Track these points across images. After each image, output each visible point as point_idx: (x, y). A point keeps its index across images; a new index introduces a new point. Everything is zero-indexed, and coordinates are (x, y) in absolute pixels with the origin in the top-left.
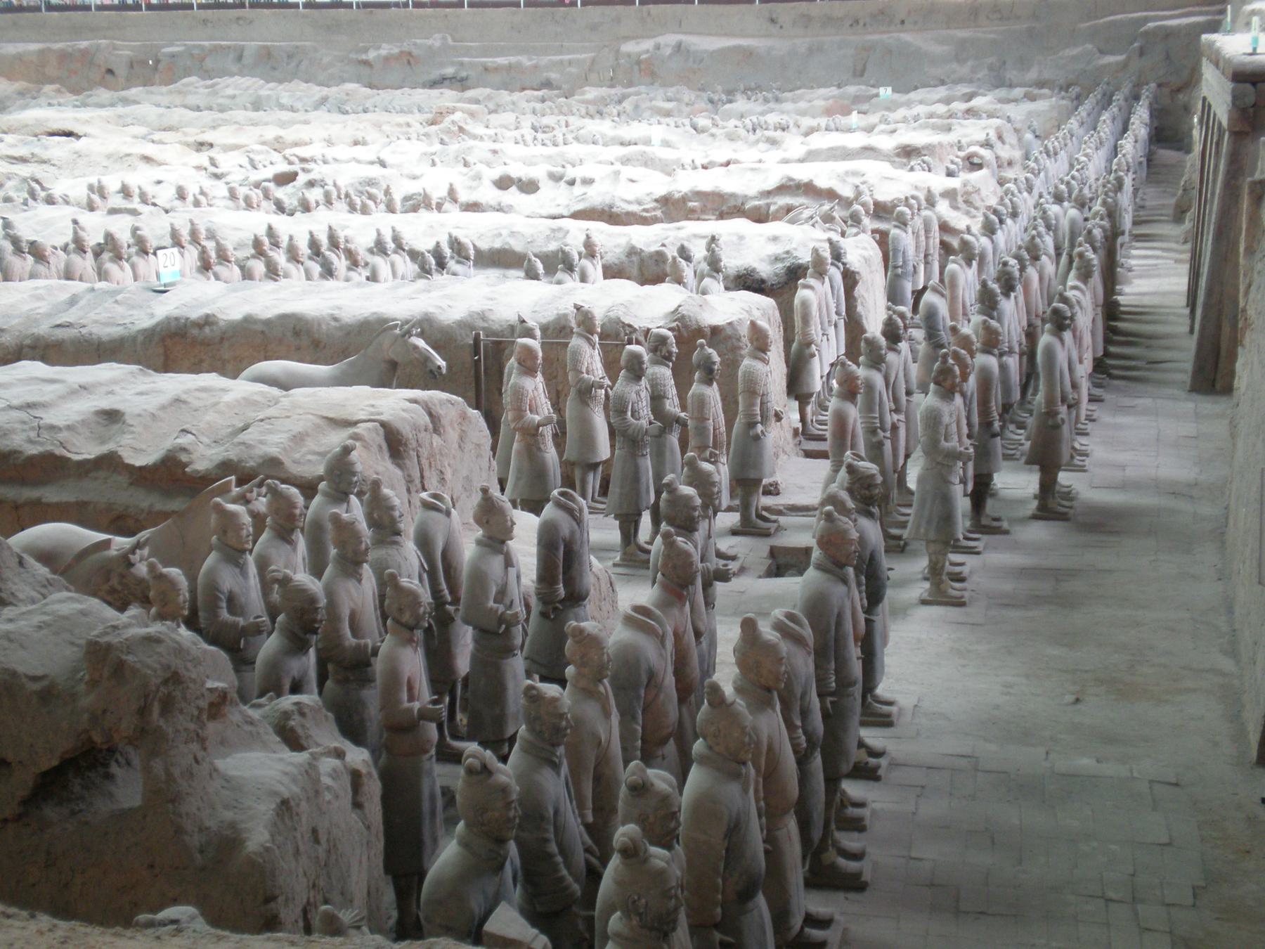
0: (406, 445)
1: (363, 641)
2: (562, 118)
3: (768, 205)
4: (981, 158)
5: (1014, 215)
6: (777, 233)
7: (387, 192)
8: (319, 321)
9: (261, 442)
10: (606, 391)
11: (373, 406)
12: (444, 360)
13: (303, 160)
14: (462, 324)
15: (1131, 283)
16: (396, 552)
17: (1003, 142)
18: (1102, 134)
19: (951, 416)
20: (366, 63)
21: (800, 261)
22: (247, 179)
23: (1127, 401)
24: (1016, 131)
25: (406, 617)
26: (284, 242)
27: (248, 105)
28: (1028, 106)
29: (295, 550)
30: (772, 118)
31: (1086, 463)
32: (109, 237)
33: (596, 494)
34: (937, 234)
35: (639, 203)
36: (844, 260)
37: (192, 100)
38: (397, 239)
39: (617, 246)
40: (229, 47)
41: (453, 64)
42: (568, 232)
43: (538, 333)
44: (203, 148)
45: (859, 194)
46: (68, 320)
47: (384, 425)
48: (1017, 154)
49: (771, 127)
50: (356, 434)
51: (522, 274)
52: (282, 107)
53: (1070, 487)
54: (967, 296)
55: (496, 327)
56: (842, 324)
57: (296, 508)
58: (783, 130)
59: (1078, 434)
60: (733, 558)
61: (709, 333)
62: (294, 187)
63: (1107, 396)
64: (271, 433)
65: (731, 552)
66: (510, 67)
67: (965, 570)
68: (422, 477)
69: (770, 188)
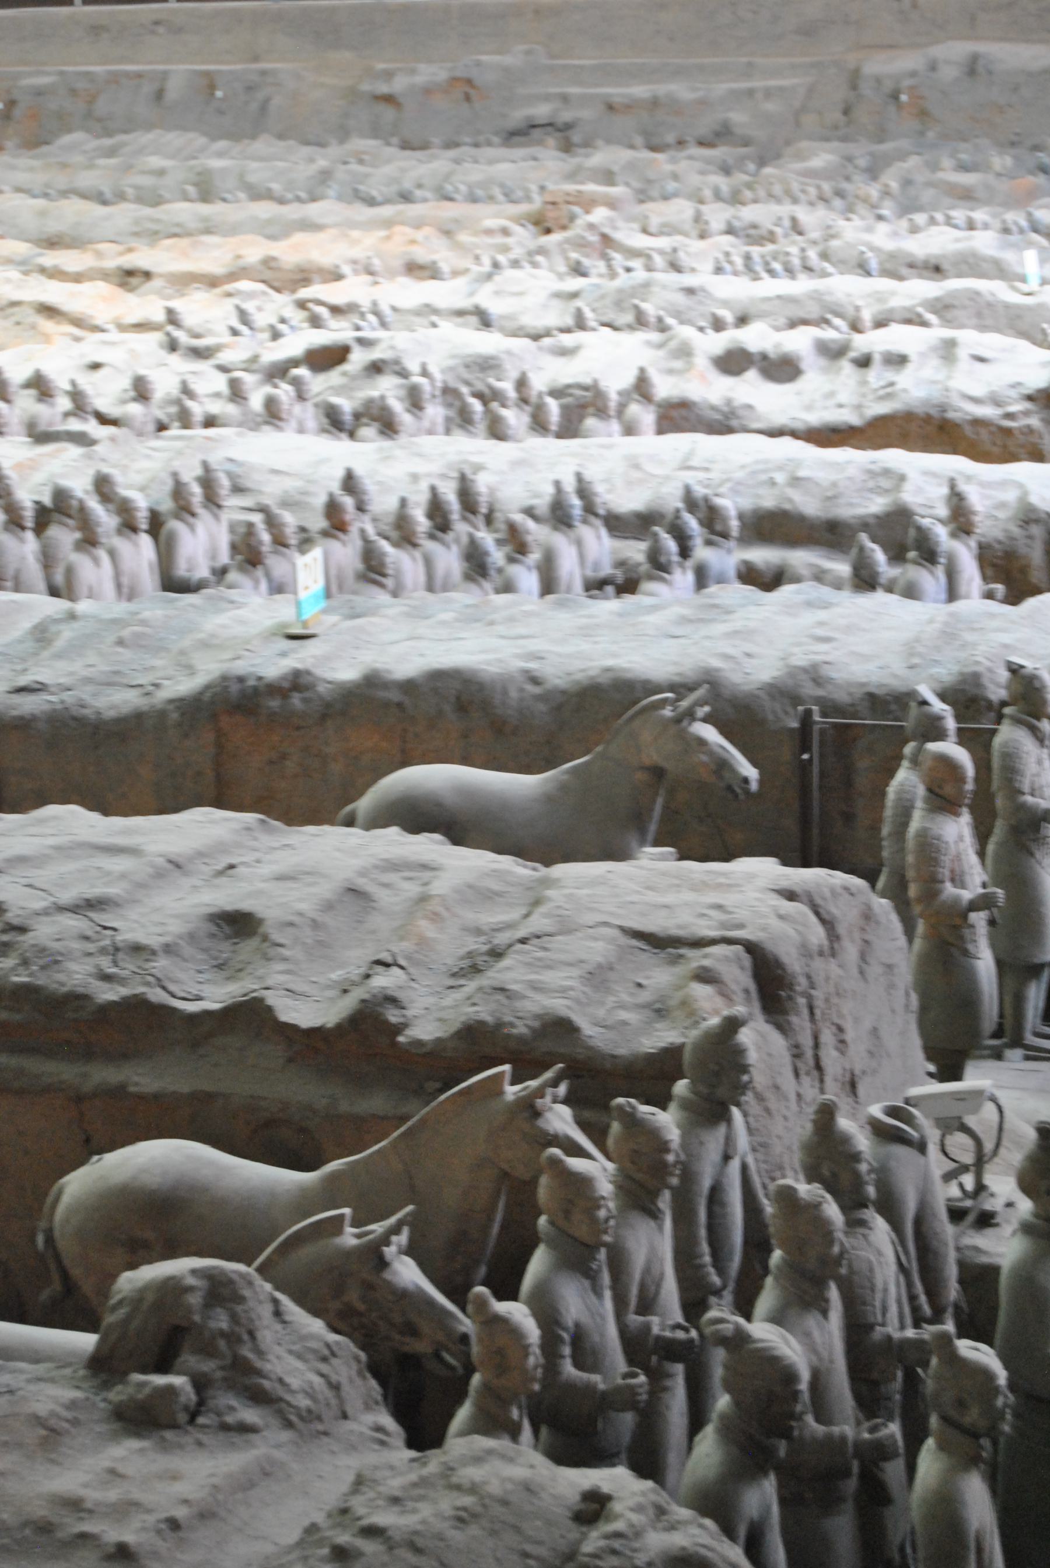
0: (790, 987)
1: (836, 1430)
2: (785, 210)
7: (522, 384)
8: (504, 683)
9: (536, 987)
11: (719, 907)
12: (755, 763)
13: (336, 310)
16: (862, 1242)
20: (389, 99)
22: (255, 359)
25: (973, 1416)
26: (384, 504)
27: (191, 190)
29: (661, 1228)
32: (61, 496)
33: (1038, 1021)
35: (996, 401)
37: (87, 179)
38: (584, 491)
39: (1002, 505)
40: (139, 75)
41: (547, 98)
42: (902, 478)
43: (951, 724)
44: (134, 281)
46: (40, 678)
47: (751, 948)
50: (704, 969)
51: (842, 568)
52: (258, 194)
55: (842, 697)
57: (667, 1150)
62: (344, 374)
64: (549, 967)
66: (655, 103)
68: (817, 1045)
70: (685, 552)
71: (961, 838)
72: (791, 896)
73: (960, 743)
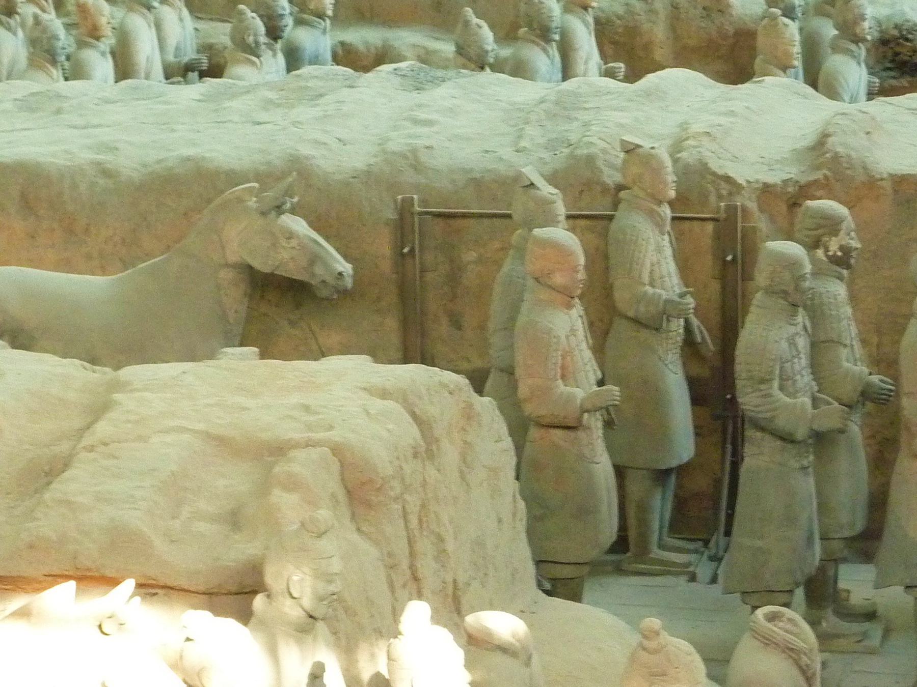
10: (687, 321)
11: (307, 408)
14: (368, 176)
33: (666, 530)
43: (561, 210)
51: (447, 48)
61: (889, 190)
68: (412, 554)
70: (274, 33)
71: (573, 331)
72: (384, 394)
73: (572, 229)
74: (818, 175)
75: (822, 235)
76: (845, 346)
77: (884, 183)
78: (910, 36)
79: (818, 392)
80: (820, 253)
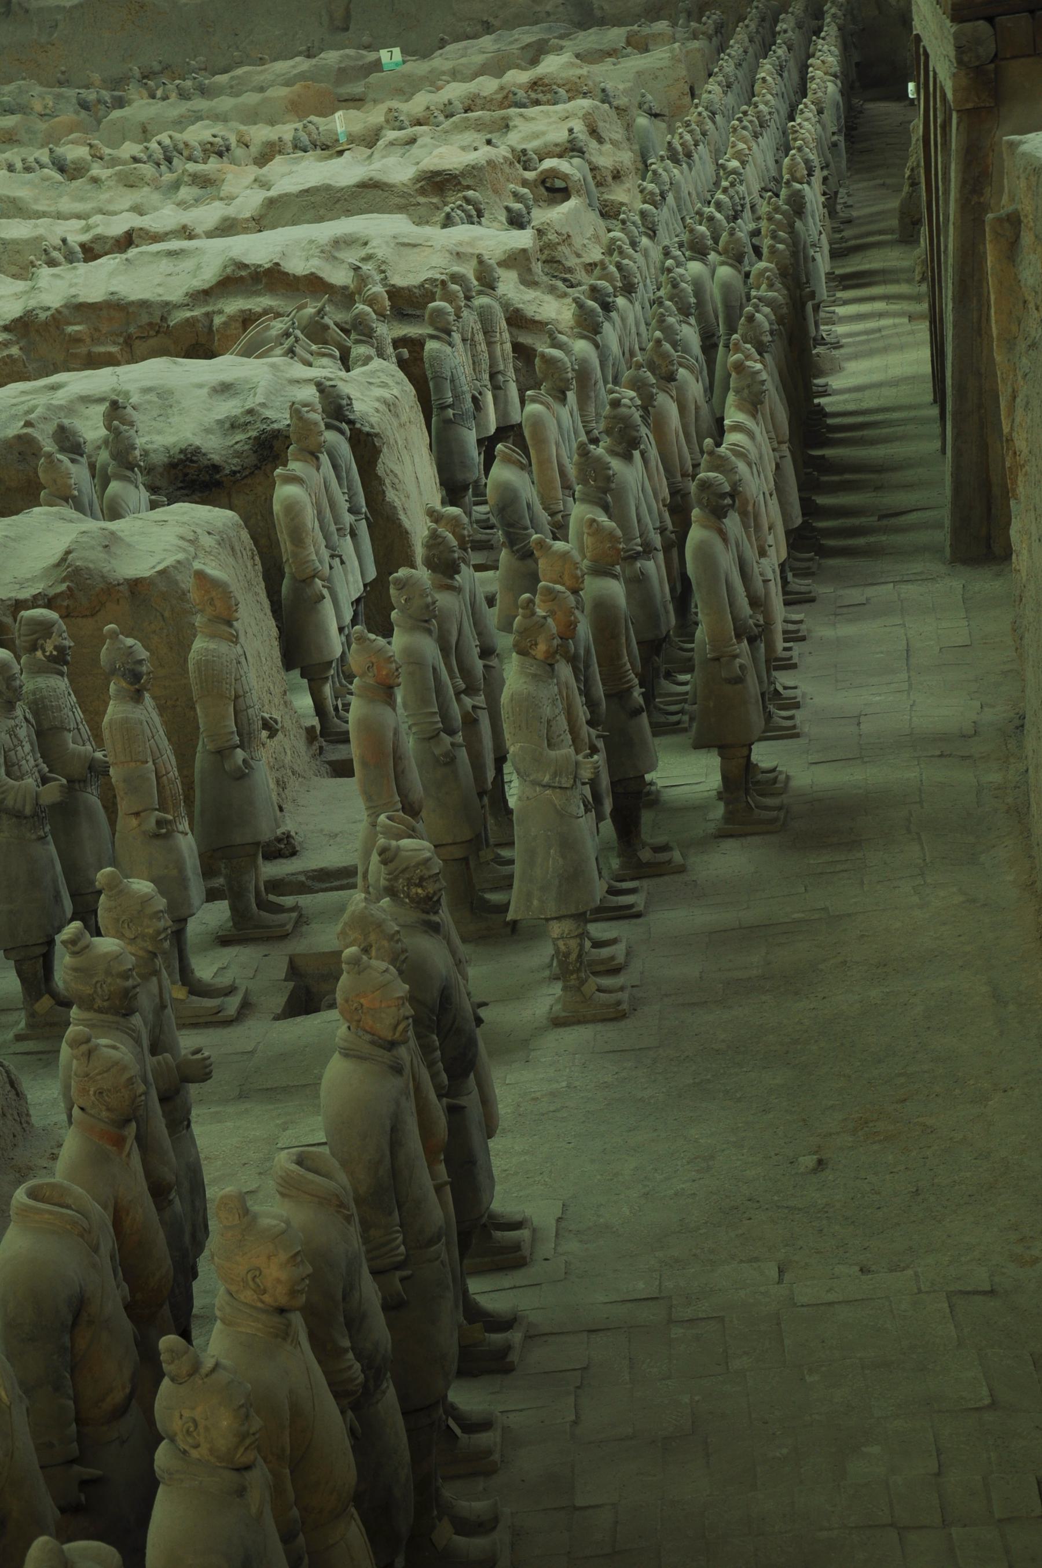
3: (209, 315)
4: (565, 177)
5: (628, 289)
6: (227, 377)
15: (841, 369)
17: (600, 140)
18: (762, 107)
19: (554, 703)
21: (275, 426)
23: (854, 595)
24: (621, 111)
28: (637, 62)
30: (197, 134)
31: (798, 721)
34: (506, 336)
36: (352, 417)
45: (362, 280)
48: (626, 158)
49: (198, 153)
53: (774, 770)
54: (564, 454)
56: (363, 527)
58: (220, 154)
59: (777, 668)
60: (230, 991)
63: (823, 590)
65: (225, 980)
67: (618, 951)
69: (206, 286)
74: (63, 587)
75: (37, 639)
76: (69, 731)
77: (121, 588)
78: (194, 458)
79: (50, 772)
80: (39, 654)
